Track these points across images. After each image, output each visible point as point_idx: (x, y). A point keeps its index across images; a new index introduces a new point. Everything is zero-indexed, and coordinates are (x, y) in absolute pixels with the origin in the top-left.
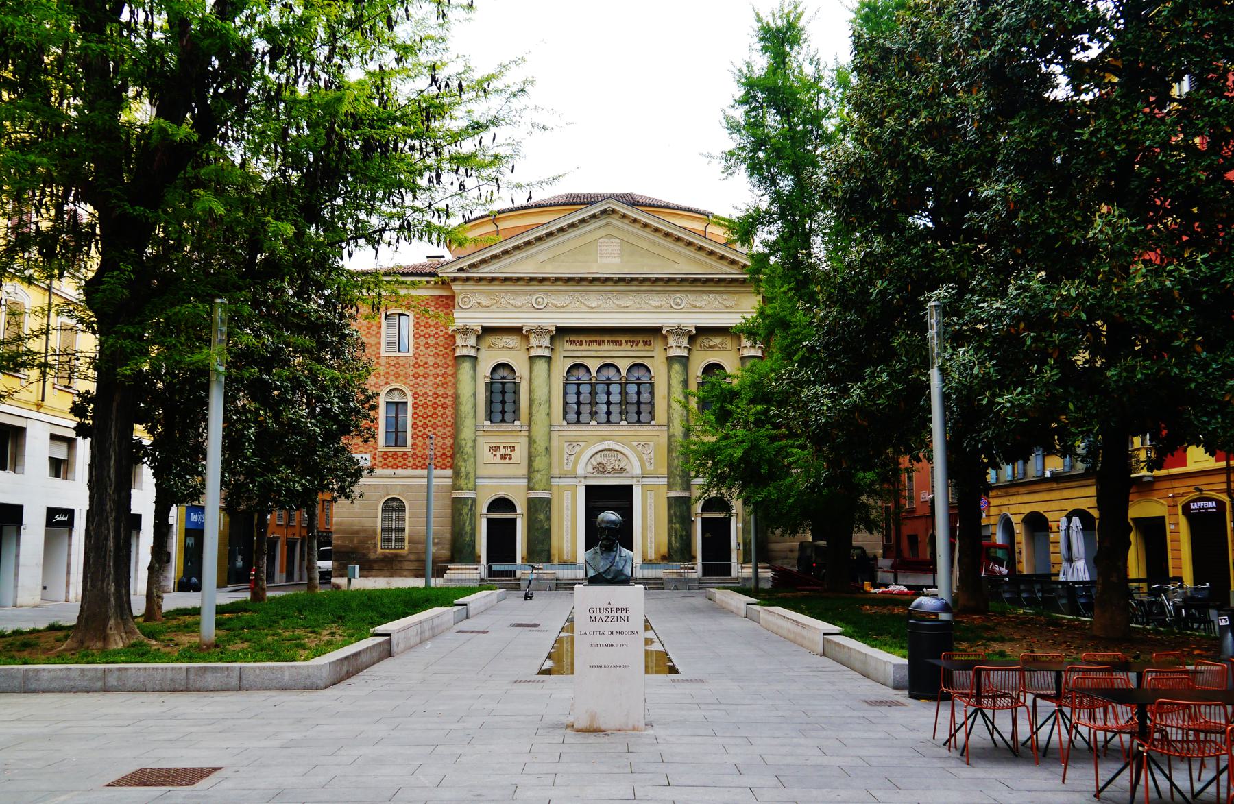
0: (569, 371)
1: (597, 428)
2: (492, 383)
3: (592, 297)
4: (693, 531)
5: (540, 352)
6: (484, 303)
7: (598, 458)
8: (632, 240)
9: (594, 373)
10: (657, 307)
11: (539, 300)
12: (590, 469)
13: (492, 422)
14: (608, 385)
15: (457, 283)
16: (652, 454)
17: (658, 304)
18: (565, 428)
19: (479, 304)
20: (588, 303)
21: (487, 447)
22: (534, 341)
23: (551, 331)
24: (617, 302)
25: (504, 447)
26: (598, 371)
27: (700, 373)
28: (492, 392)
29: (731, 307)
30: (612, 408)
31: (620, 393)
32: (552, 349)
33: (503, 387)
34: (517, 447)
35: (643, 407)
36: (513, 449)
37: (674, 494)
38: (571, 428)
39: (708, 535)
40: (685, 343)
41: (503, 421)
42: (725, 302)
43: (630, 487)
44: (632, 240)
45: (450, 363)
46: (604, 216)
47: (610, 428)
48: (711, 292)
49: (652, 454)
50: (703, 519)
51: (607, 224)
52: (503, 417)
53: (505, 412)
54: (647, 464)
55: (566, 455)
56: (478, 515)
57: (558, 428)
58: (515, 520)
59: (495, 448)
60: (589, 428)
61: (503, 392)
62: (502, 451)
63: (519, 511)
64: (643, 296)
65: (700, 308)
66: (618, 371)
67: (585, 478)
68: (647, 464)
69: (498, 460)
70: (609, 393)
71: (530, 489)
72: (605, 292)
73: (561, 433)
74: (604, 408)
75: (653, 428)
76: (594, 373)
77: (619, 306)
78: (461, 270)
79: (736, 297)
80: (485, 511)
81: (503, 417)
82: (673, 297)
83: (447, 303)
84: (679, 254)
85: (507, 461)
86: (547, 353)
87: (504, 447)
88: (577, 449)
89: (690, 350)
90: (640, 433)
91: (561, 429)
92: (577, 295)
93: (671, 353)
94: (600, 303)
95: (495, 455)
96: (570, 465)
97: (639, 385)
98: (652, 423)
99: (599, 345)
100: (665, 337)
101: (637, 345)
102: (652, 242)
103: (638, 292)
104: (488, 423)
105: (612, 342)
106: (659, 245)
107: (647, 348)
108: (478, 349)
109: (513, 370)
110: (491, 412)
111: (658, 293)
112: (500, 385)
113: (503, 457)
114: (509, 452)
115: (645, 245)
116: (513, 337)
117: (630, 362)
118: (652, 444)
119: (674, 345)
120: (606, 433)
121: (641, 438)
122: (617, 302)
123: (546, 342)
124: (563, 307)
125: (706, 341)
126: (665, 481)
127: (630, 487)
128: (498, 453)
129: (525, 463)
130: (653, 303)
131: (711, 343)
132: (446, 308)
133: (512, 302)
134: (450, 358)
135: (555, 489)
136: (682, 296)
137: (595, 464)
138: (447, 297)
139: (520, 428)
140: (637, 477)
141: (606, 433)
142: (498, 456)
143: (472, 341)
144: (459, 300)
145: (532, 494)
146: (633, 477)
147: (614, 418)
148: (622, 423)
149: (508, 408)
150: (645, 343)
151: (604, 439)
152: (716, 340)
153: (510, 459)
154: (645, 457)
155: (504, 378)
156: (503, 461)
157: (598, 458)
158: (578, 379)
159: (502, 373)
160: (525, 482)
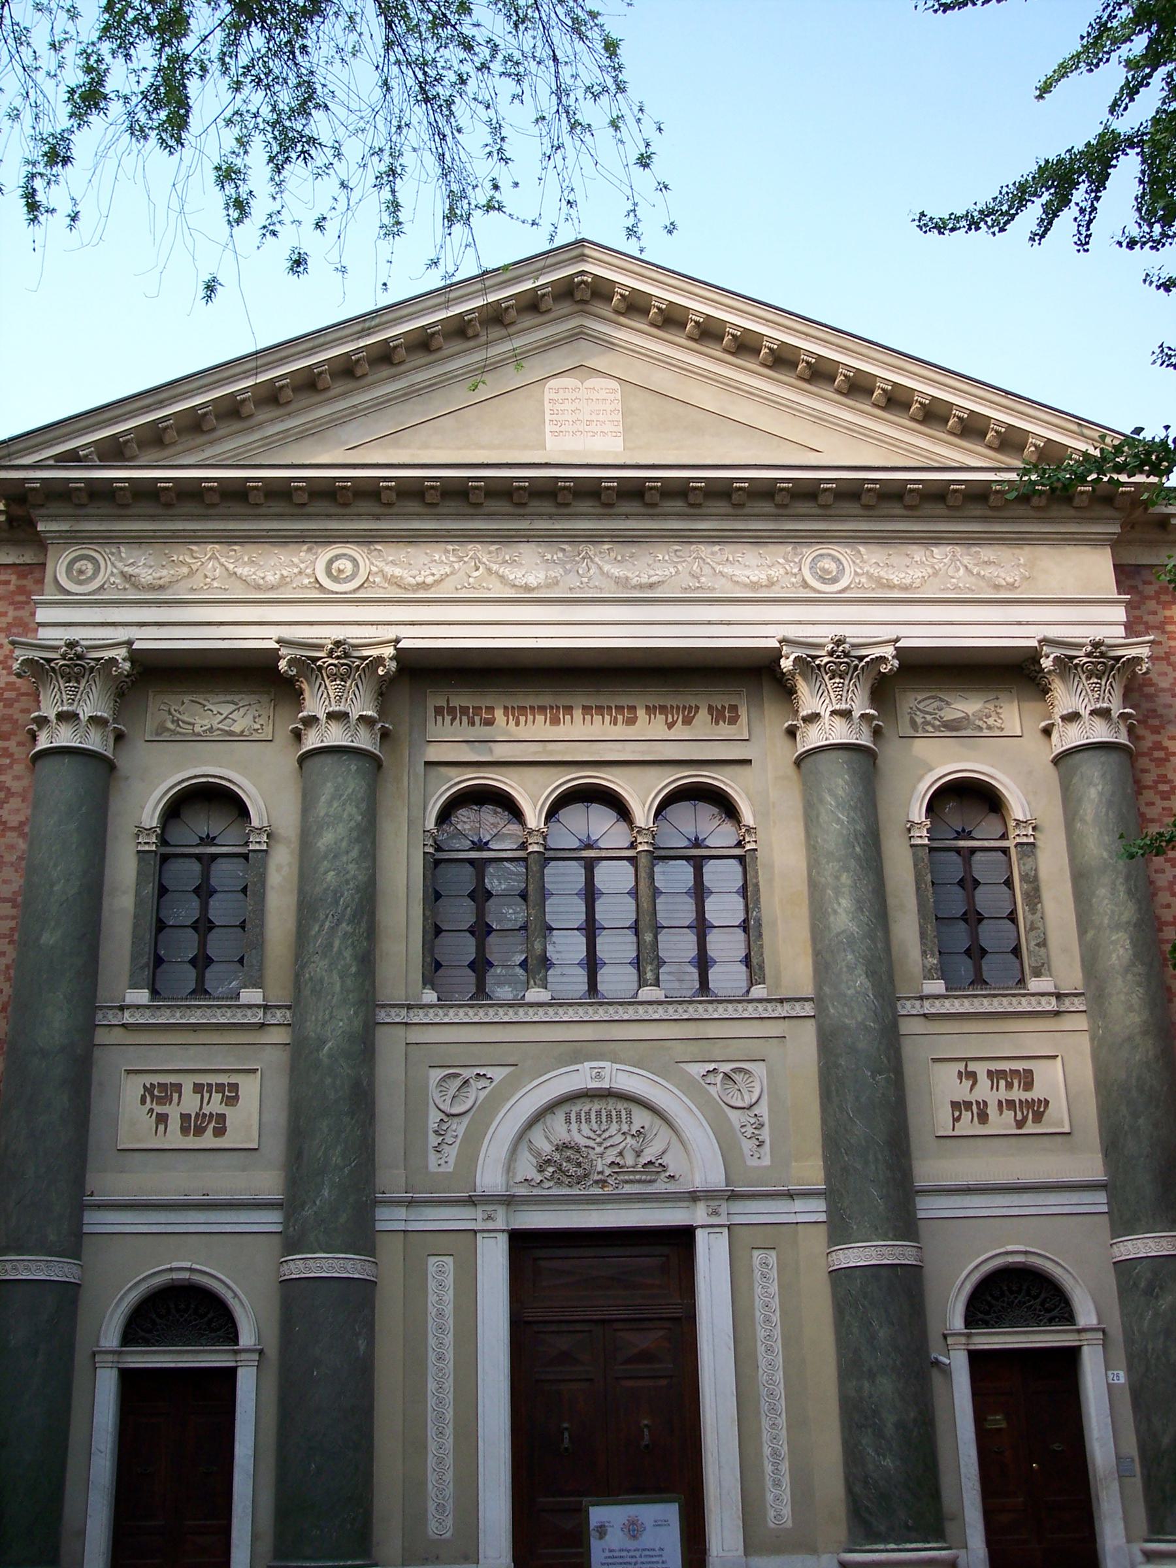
0: (445, 816)
1: (551, 1014)
2: (165, 859)
3: (528, 553)
4: (940, 1403)
5: (335, 736)
6: (146, 575)
7: (559, 1128)
8: (661, 379)
9: (534, 818)
10: (754, 586)
11: (345, 565)
12: (527, 1168)
13: (155, 993)
14: (590, 866)
15: (53, 509)
16: (763, 1109)
17: (758, 575)
18: (431, 1016)
19: (127, 577)
20: (511, 573)
21: (133, 1088)
22: (315, 704)
23: (379, 661)
24: (616, 571)
25: (198, 1088)
26: (552, 813)
27: (918, 812)
28: (163, 891)
29: (1012, 587)
30: (606, 946)
31: (635, 893)
32: (385, 735)
33: (206, 875)
34: (249, 1088)
35: (717, 943)
36: (231, 1095)
37: (856, 1255)
38: (452, 1016)
39: (998, 1420)
40: (860, 705)
41: (200, 990)
42: (986, 572)
43: (684, 1237)
44: (661, 379)
45: (16, 786)
46: (565, 307)
47: (601, 1013)
48: (936, 539)
49: (763, 1109)
50: (976, 1358)
51: (578, 335)
52: (201, 980)
53: (209, 961)
54: (748, 1146)
55: (434, 1117)
56: (81, 1358)
57: (401, 1016)
58: (229, 1375)
59: (165, 1093)
60: (522, 1015)
61: (204, 891)
62: (190, 1103)
63: (247, 1338)
64: (704, 550)
65: (906, 588)
66: (622, 811)
67: (509, 1201)
68: (748, 1146)
69: (174, 1137)
70: (590, 894)
71: (292, 1243)
72: (574, 538)
73: (415, 1035)
74: (576, 946)
75: (761, 1010)
76: (534, 818)
77: (623, 582)
78: (71, 458)
79: (1024, 554)
80: (111, 1338)
81: (201, 980)
82: (809, 553)
83: (21, 590)
84: (820, 419)
85: (208, 1140)
86: (364, 740)
87: (198, 1088)
88: (476, 1094)
89: (877, 733)
90: (712, 1031)
91: (418, 1017)
92: (473, 549)
93: (813, 737)
94: (554, 573)
95: (162, 1119)
96: (452, 1153)
97: (698, 864)
98: (758, 991)
99: (555, 721)
100: (786, 690)
101: (688, 721)
102: (728, 385)
103: (686, 538)
104: (141, 996)
105: (600, 709)
106: (751, 394)
107: (725, 730)
108: (119, 737)
109: (243, 812)
110: (159, 961)
111: (758, 540)
112: (196, 867)
113: (192, 1125)
114: (215, 1105)
115: (706, 397)
116: (246, 699)
117: (665, 781)
118: (758, 1069)
119: (825, 711)
120: (587, 1033)
121: (717, 1051)
122: (616, 571)
123: (361, 706)
124: (423, 586)
125: (931, 706)
126: (814, 1210)
127: (684, 1237)
128: (173, 1112)
129: (276, 1149)
130: (740, 573)
131: (949, 715)
132: (18, 606)
133: (243, 571)
134: (19, 768)
135: (391, 1253)
136: (842, 552)
137: (546, 1148)
138: (22, 570)
139: (258, 1017)
140: (708, 1195)
141: (587, 1033)
142: (174, 1123)
143: (92, 704)
144: (59, 566)
145: (304, 1266)
146: (694, 1197)
147: (608, 980)
148: (647, 993)
149: (217, 945)
150: (717, 715)
151: (577, 1053)
152: (966, 706)
153: (220, 1132)
154: (733, 1115)
155: (209, 840)
156: (191, 1142)
157: (559, 1128)
158: (481, 846)
159: (201, 823)
160: (271, 1220)
